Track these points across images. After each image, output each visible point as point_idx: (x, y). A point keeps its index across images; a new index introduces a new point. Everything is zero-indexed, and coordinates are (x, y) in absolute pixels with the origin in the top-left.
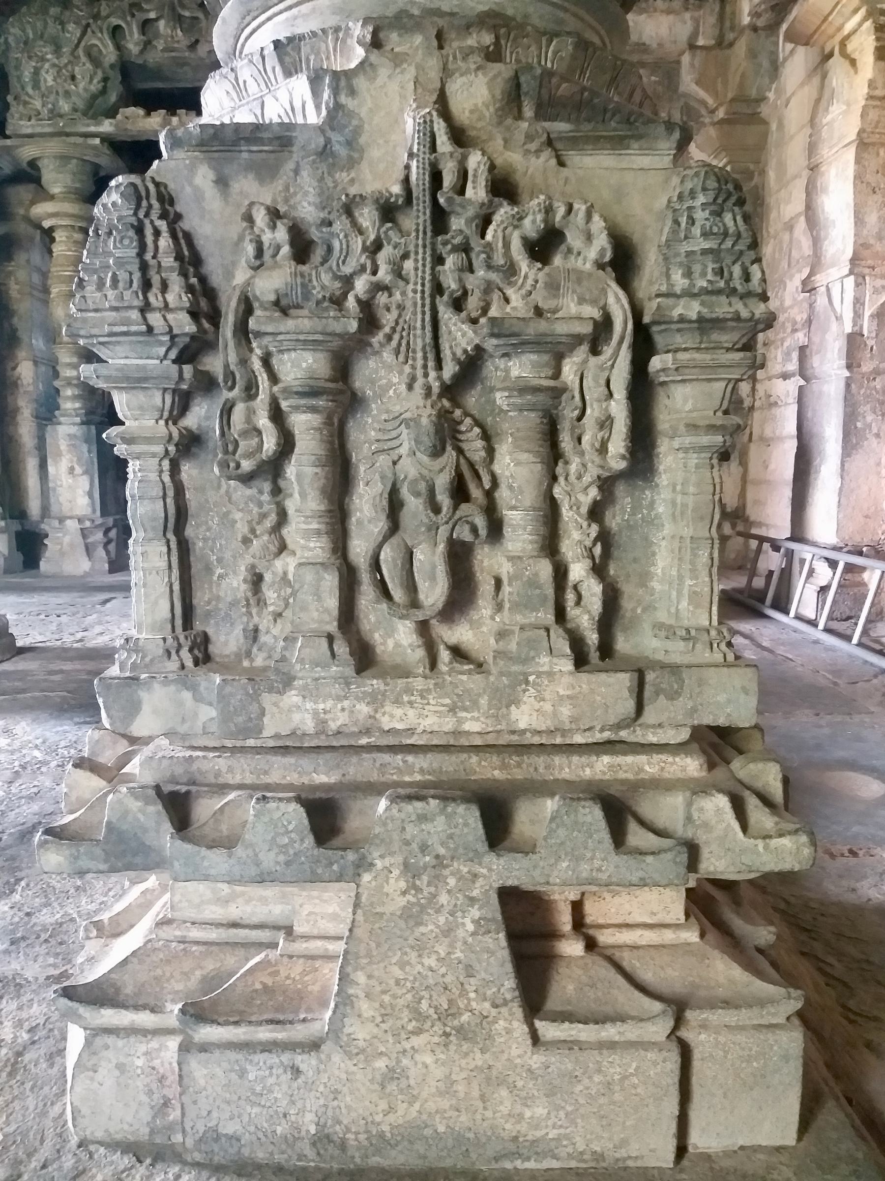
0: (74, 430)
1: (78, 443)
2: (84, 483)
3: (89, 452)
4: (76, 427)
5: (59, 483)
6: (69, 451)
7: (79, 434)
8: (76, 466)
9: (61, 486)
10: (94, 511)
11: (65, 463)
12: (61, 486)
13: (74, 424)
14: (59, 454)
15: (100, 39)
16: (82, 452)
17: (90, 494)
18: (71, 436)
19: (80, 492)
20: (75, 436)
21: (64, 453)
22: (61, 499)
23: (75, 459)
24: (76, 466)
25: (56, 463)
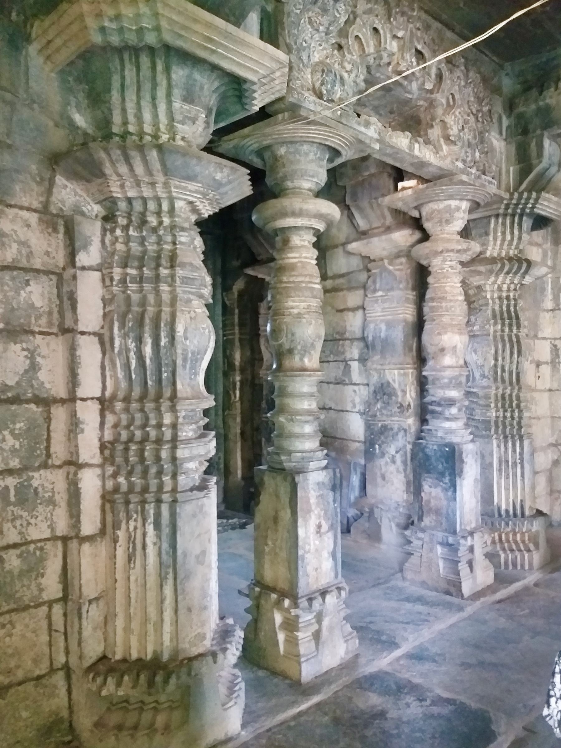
3: (334, 501)
4: (324, 473)
5: (307, 548)
7: (326, 480)
10: (336, 576)
11: (313, 521)
12: (309, 552)
14: (309, 511)
15: (363, 34)
16: (328, 503)
17: (334, 555)
19: (325, 554)
20: (323, 483)
21: (313, 507)
22: (309, 569)
25: (306, 521)
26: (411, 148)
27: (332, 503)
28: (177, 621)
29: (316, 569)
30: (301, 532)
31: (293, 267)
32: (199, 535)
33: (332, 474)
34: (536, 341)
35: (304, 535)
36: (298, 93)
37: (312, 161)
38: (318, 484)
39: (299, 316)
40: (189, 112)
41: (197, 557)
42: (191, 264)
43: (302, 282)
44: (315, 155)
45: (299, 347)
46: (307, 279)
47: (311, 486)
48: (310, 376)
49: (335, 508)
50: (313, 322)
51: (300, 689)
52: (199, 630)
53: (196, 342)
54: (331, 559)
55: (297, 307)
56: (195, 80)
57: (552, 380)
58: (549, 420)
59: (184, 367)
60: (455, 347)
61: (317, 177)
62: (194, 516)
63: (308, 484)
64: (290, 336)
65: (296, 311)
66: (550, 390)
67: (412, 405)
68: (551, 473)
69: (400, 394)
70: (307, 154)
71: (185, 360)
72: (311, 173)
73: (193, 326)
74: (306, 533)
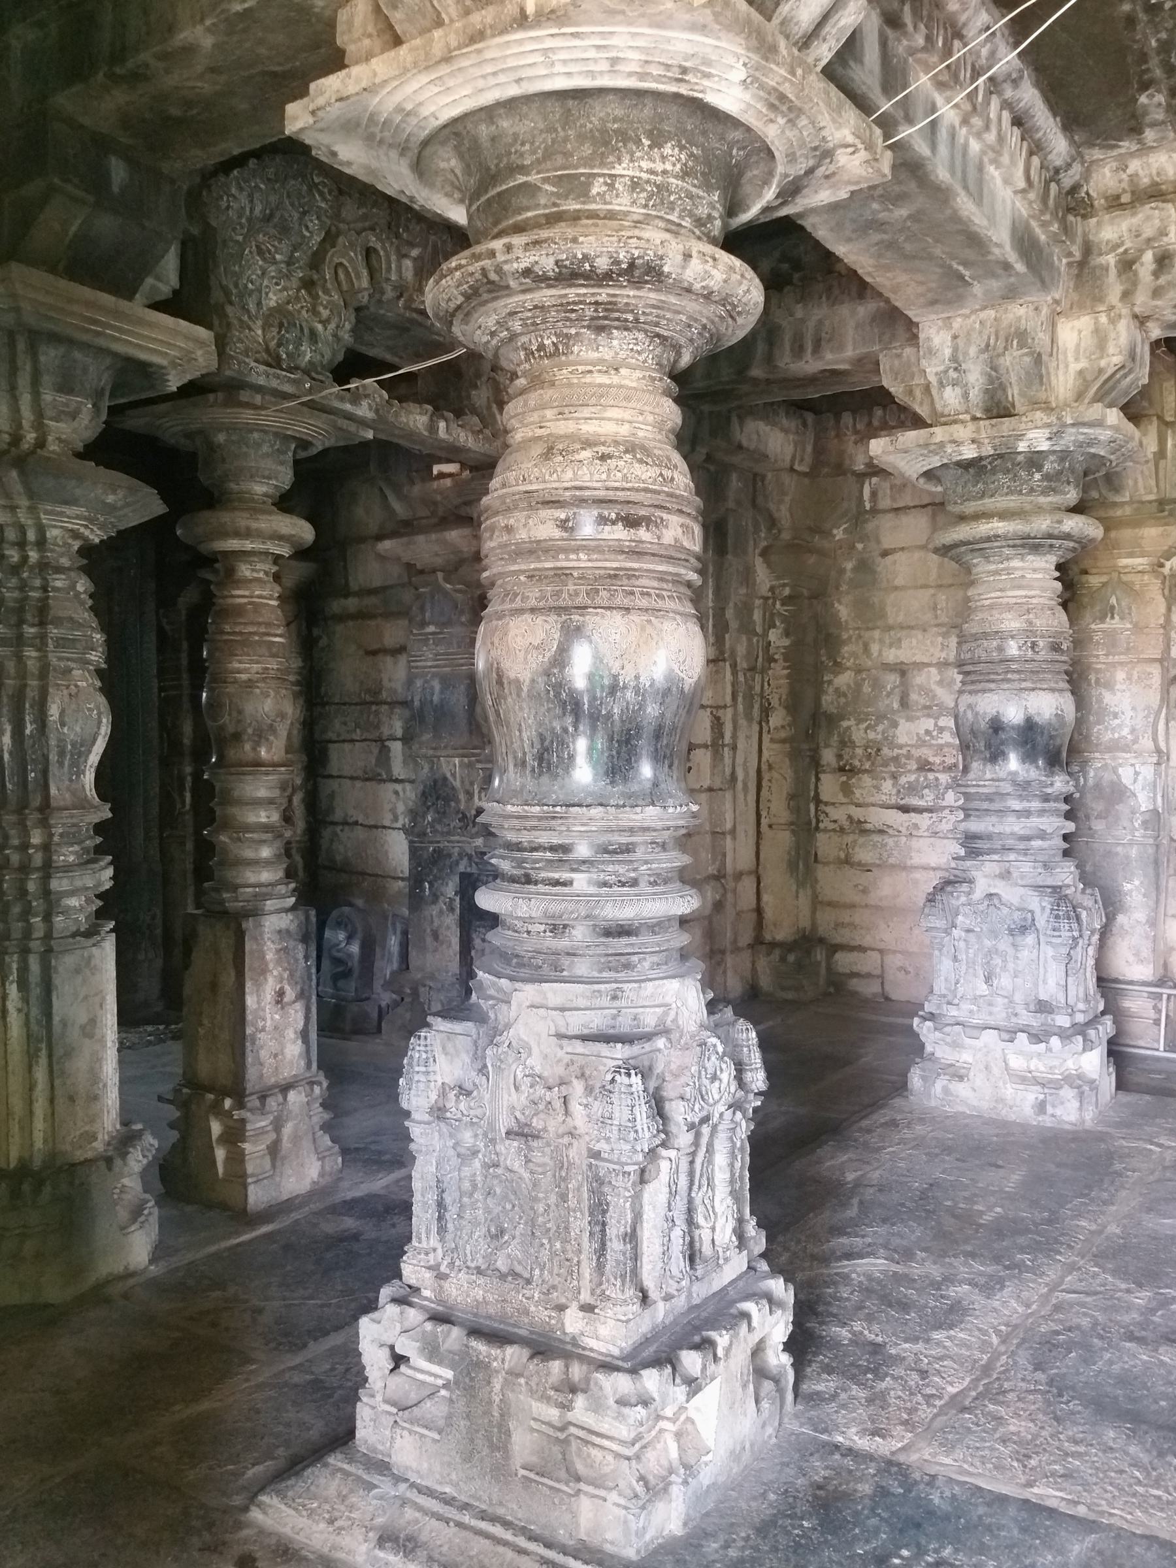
0: (285, 921)
1: (292, 943)
2: (296, 1016)
3: (306, 958)
4: (290, 916)
5: (261, 1024)
6: (279, 962)
7: (293, 927)
8: (287, 988)
9: (263, 1030)
10: (309, 1065)
11: (270, 986)
12: (263, 1030)
13: (287, 911)
14: (264, 971)
15: (351, 260)
16: (297, 960)
17: (304, 1035)
18: (282, 933)
19: (290, 1034)
20: (288, 931)
21: (271, 966)
22: (263, 1053)
23: (286, 975)
24: (287, 988)
25: (259, 986)
26: (432, 428)
27: (302, 961)
28: (53, 1114)
29: (276, 1056)
30: (250, 1001)
31: (239, 611)
32: (86, 997)
33: (303, 918)
35: (255, 1006)
36: (239, 363)
37: (267, 455)
38: (280, 932)
39: (250, 684)
40: (67, 405)
41: (83, 1028)
42: (71, 619)
43: (254, 633)
44: (272, 446)
45: (250, 731)
46: (263, 630)
47: (266, 936)
48: (267, 774)
49: (309, 967)
50: (272, 693)
51: (243, 1217)
52: (87, 1128)
53: (78, 729)
54: (299, 1042)
55: (246, 671)
56: (75, 361)
57: (713, 774)
58: (708, 838)
59: (61, 764)
61: (276, 478)
62: (78, 971)
63: (262, 934)
64: (234, 714)
65: (244, 677)
66: (710, 790)
68: (710, 923)
69: (462, 796)
70: (258, 445)
71: (62, 753)
72: (267, 473)
73: (73, 706)
74: (258, 1003)
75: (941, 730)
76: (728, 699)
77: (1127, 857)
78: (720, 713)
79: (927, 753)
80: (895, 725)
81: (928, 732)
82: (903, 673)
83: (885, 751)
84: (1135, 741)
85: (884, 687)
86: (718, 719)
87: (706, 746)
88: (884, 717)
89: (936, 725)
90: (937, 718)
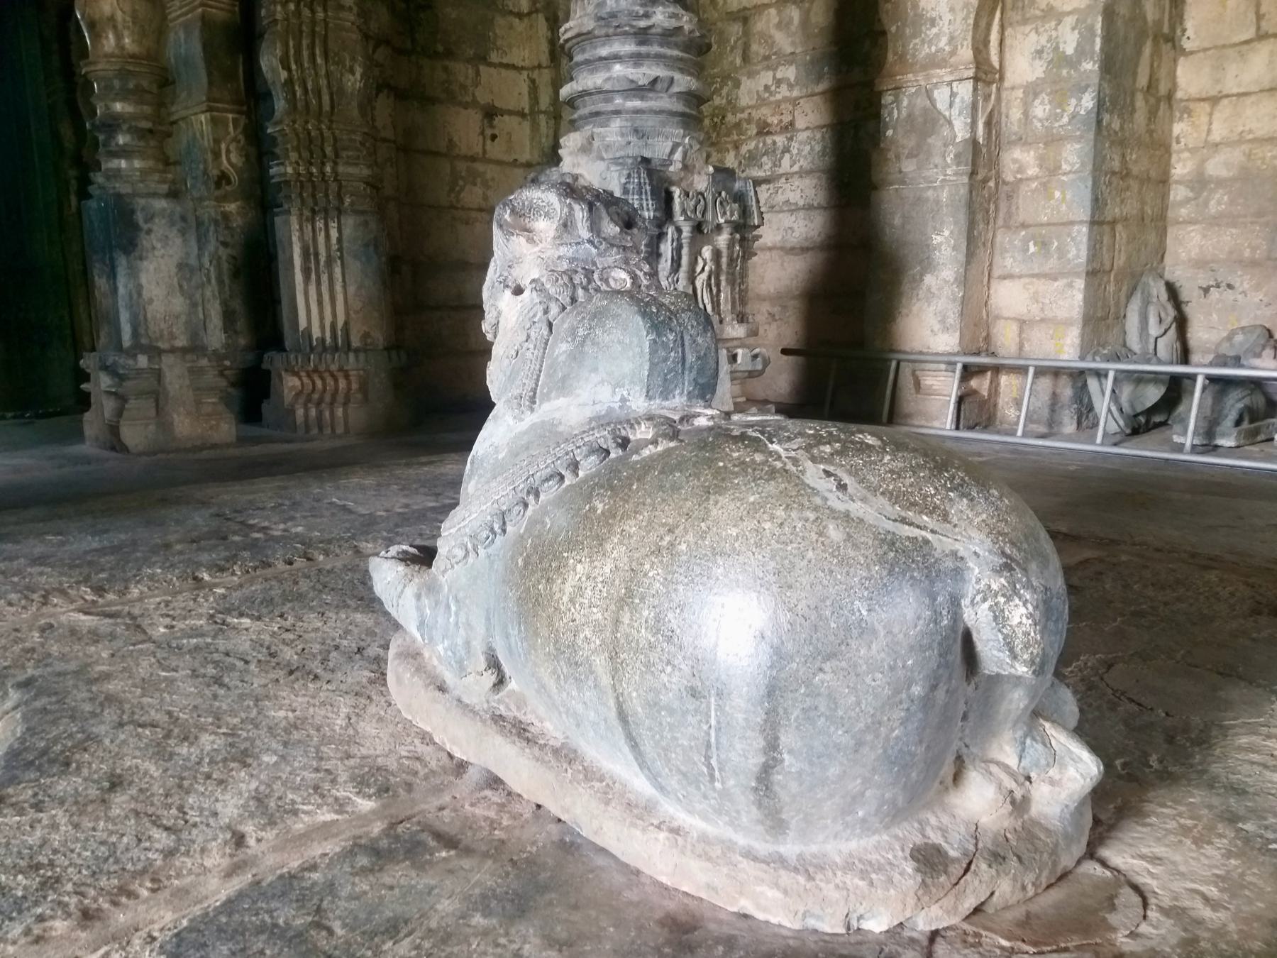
34: (482, 68)
60: (112, 18)
67: (234, 177)
75: (778, 82)
76: (545, 59)
77: (937, 202)
78: (535, 75)
79: (765, 113)
80: (737, 85)
81: (767, 88)
82: (745, 21)
83: (730, 118)
84: (953, 53)
85: (728, 41)
86: (533, 81)
87: (522, 115)
88: (729, 77)
89: (774, 77)
90: (775, 70)
